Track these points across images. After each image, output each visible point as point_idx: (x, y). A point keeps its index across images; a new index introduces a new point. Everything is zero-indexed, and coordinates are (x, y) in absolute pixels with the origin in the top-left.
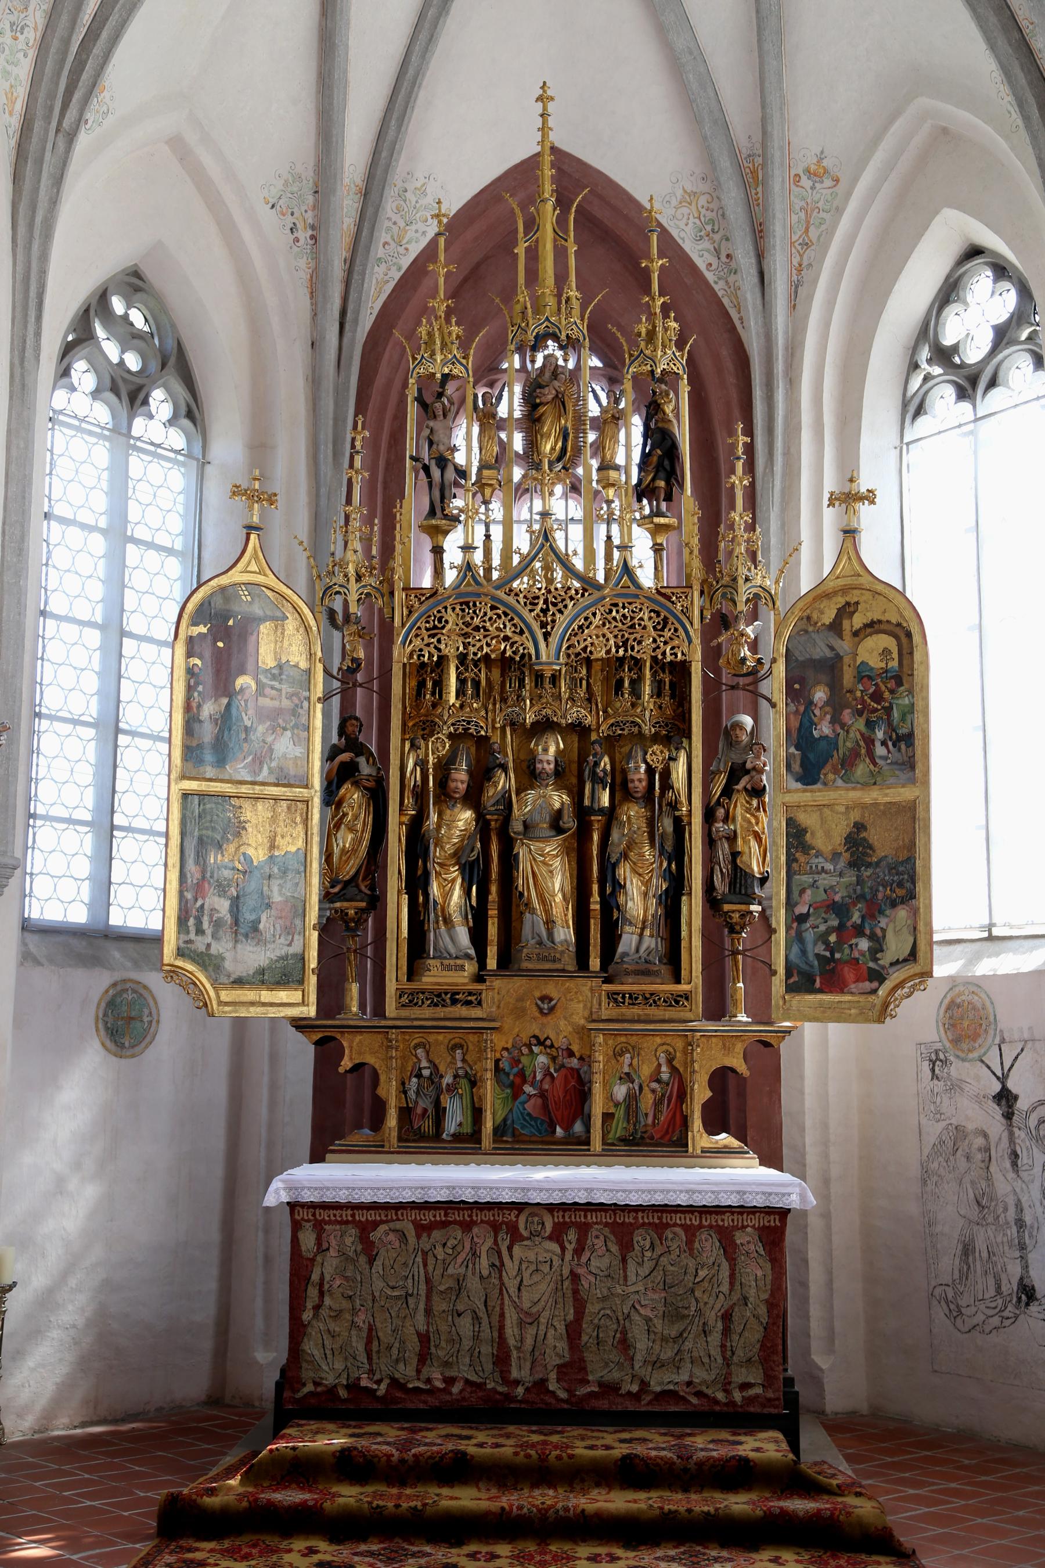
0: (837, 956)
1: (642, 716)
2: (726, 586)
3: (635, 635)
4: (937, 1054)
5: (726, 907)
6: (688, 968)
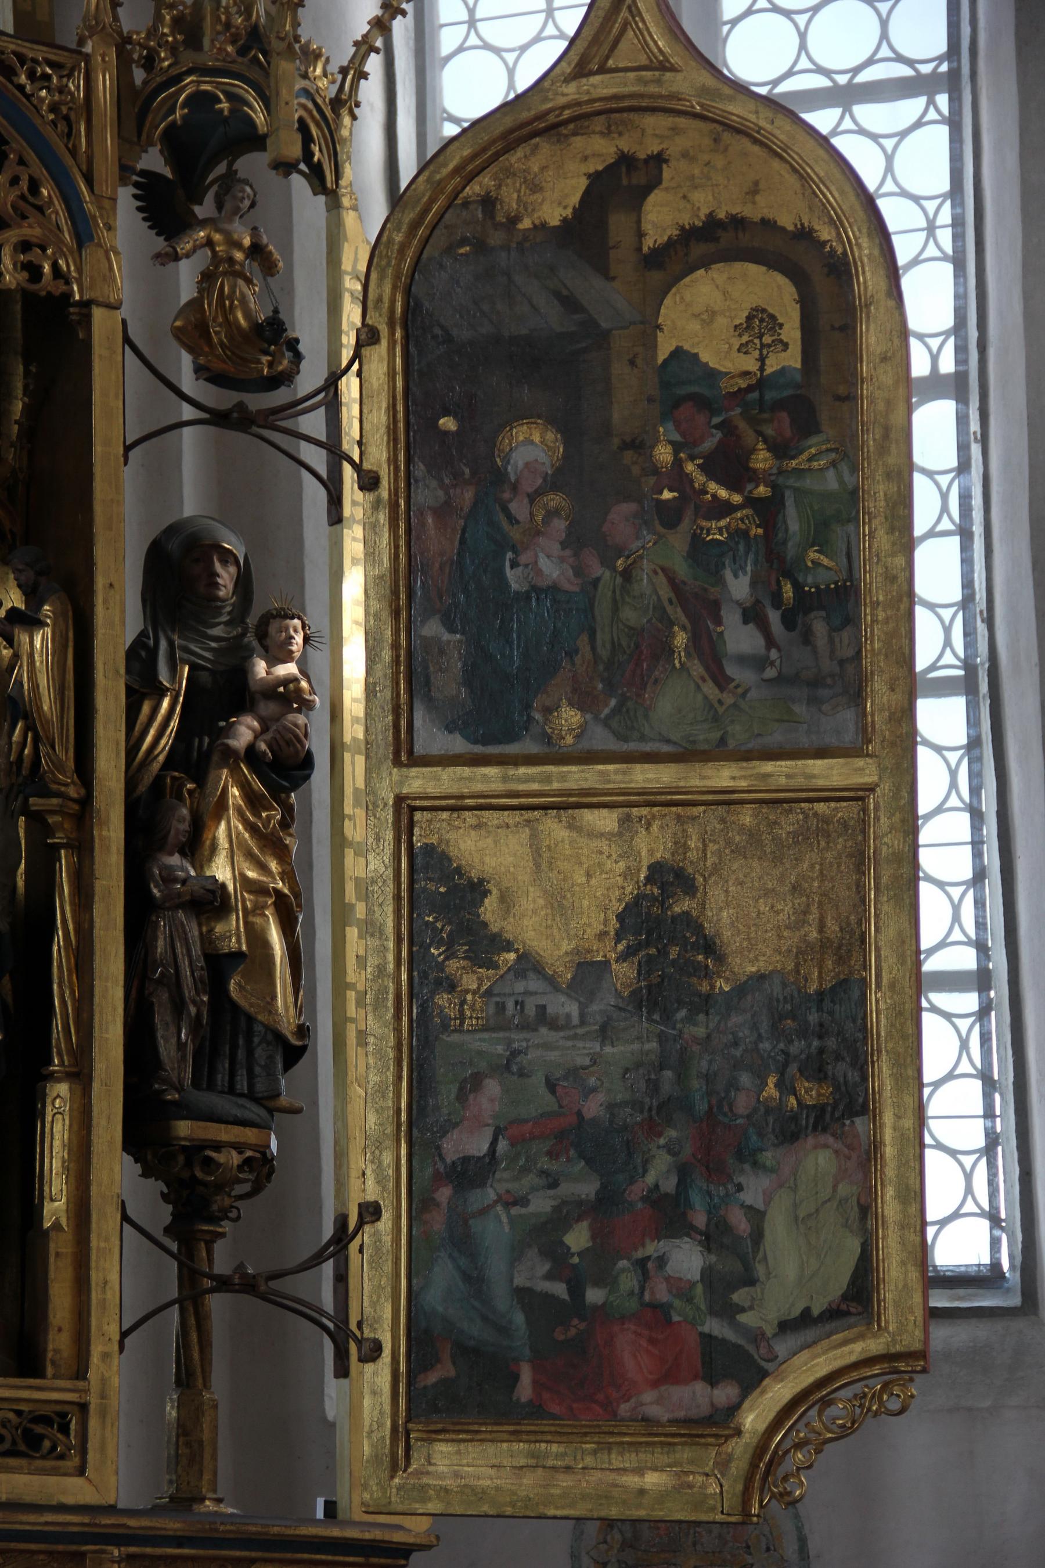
0: (594, 1296)
5: (184, 1128)
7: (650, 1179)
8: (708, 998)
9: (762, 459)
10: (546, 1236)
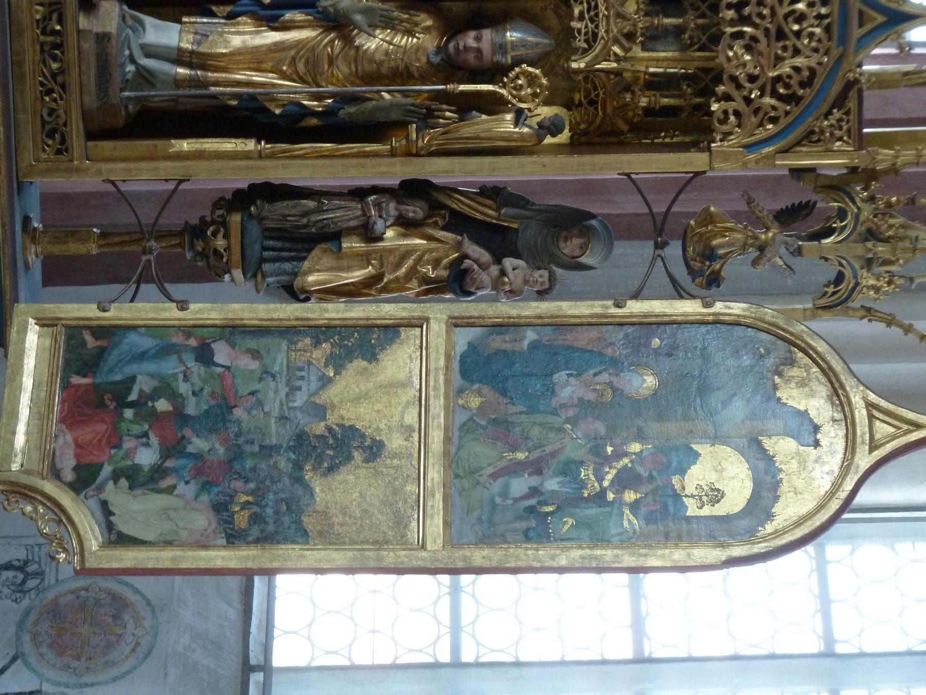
1: (607, 55)
2: (857, 217)
3: (763, 41)
4: (36, 574)
6: (116, 154)
7: (195, 440)
8: (301, 468)
9: (630, 496)
10: (165, 389)
